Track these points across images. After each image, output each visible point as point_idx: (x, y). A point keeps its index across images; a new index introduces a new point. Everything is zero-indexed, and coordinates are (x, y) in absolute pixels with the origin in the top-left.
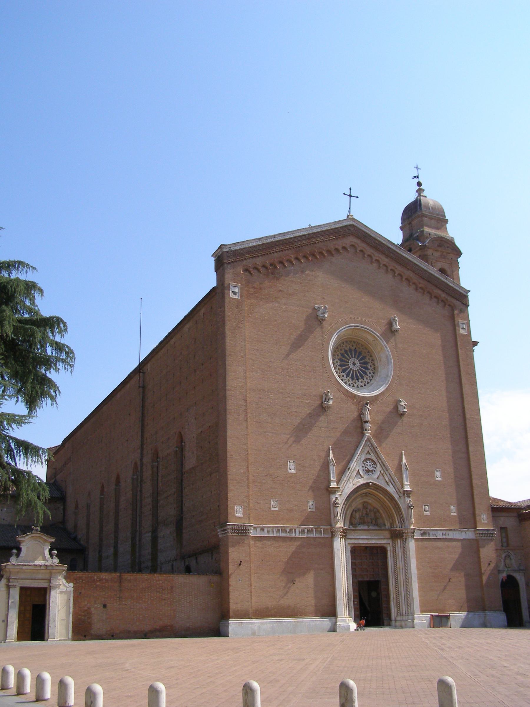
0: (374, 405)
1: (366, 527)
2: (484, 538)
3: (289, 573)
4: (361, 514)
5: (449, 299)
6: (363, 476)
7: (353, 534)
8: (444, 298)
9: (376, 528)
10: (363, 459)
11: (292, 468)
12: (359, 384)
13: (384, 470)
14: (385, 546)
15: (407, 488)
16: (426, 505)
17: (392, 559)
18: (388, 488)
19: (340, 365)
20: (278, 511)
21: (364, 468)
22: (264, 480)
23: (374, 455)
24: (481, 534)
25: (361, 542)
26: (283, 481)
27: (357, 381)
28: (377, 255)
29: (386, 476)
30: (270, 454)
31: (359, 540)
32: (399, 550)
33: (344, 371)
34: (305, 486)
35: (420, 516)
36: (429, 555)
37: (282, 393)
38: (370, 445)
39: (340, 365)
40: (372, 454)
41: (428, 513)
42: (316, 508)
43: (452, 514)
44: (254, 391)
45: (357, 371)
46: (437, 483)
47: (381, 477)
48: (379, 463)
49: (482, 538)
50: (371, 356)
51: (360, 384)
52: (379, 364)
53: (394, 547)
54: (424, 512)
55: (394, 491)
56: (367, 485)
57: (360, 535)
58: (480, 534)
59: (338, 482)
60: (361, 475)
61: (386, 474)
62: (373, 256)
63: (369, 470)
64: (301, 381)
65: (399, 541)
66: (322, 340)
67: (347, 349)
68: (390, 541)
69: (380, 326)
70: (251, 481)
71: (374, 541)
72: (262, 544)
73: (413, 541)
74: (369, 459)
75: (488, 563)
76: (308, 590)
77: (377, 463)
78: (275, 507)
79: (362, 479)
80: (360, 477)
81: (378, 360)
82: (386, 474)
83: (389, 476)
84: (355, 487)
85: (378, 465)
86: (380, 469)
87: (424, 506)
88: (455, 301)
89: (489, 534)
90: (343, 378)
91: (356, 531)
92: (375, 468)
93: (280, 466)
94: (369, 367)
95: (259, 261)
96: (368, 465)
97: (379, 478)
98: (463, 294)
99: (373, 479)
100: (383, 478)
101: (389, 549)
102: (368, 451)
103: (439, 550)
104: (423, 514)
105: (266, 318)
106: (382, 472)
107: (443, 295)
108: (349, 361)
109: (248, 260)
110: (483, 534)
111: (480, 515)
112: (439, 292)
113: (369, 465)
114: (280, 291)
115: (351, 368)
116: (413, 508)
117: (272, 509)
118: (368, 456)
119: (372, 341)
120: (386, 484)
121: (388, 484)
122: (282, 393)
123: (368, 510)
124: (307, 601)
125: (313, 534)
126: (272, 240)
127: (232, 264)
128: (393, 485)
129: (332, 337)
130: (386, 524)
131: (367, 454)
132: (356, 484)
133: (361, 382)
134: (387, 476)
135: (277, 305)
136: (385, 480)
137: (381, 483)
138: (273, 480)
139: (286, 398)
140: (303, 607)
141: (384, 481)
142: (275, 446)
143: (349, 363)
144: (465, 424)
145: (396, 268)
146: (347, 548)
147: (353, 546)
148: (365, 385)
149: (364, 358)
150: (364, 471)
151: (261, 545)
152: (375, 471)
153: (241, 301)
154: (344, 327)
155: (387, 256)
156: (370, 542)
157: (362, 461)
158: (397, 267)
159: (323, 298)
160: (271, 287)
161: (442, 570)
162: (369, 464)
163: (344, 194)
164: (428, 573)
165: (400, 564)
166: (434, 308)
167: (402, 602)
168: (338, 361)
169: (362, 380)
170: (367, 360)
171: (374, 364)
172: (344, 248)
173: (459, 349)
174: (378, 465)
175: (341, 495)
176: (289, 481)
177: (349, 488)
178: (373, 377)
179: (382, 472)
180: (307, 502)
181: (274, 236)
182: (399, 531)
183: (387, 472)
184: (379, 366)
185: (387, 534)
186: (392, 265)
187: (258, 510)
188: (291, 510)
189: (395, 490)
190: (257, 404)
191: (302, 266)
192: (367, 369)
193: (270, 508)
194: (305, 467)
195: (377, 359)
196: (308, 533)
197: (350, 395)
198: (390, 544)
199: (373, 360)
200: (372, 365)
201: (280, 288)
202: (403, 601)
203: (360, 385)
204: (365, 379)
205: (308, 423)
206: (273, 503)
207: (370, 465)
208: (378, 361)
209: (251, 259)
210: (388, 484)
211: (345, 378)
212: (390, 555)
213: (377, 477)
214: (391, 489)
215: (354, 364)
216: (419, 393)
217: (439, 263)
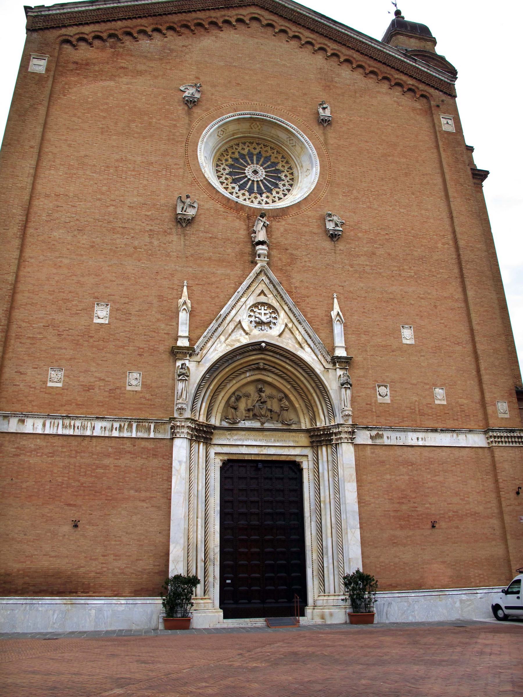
0: (279, 222)
1: (257, 425)
2: (504, 445)
3: (69, 505)
4: (249, 402)
5: (422, 86)
6: (248, 332)
7: (228, 437)
8: (413, 85)
9: (279, 426)
10: (251, 302)
12: (262, 200)
13: (293, 323)
14: (298, 459)
15: (341, 352)
16: (382, 386)
17: (312, 486)
18: (300, 353)
19: (230, 174)
20: (63, 389)
21: (253, 319)
22: (40, 333)
23: (273, 298)
24: (498, 437)
25: (244, 450)
26: (80, 337)
27: (258, 196)
28: (293, 30)
29: (297, 332)
30: (61, 292)
31: (240, 448)
32: (323, 467)
33: (234, 181)
34: (124, 346)
35: (370, 404)
36: (388, 477)
37: (99, 200)
38: (267, 281)
39: (230, 174)
40: (270, 296)
41: (388, 400)
42: (144, 385)
43: (437, 402)
44: (47, 196)
45: (260, 183)
46: (404, 349)
47: (287, 334)
48: (283, 312)
49: (500, 444)
50: (287, 162)
51: (265, 199)
52: (300, 172)
53: (317, 462)
54: (379, 397)
55: (313, 359)
57: (243, 440)
58: (495, 437)
60: (244, 330)
61: (298, 329)
62: (288, 30)
63: (262, 321)
64: (141, 184)
65: (324, 449)
66: (187, 129)
67: (245, 152)
68: (308, 451)
69: (297, 116)
70: (14, 335)
71: (272, 451)
72: (17, 448)
73: (351, 448)
74: (263, 304)
75: (515, 492)
76: (109, 541)
77: (279, 311)
79: (247, 337)
80: (243, 333)
81: (298, 166)
82: (298, 329)
83: (303, 332)
84: (229, 349)
85: (282, 314)
86: (286, 321)
87: (379, 386)
88: (432, 91)
89: (515, 437)
90: (233, 190)
91: (235, 432)
92: (275, 318)
93: (78, 312)
94: (283, 177)
95: (87, 29)
96: (259, 313)
97: (283, 336)
98: (445, 82)
100: (292, 336)
101: (307, 466)
102: (262, 290)
103: (410, 468)
104: (376, 401)
105: (89, 100)
106: (290, 325)
107: (410, 82)
108: (247, 169)
109: (70, 29)
110: (501, 437)
111: (495, 405)
112: (404, 78)
113: (263, 314)
114: (122, 68)
115: (249, 177)
116: (349, 386)
117: (50, 384)
118: (263, 299)
119: (286, 139)
120: (297, 346)
121: (302, 347)
122: (99, 200)
123: (263, 395)
124: (102, 563)
125: (131, 431)
127: (41, 32)
128: (311, 348)
129: (207, 126)
130: (302, 420)
131: (259, 295)
132: (234, 345)
133: (268, 197)
134: (300, 332)
135: (112, 83)
136: (296, 339)
138: (58, 335)
139: (108, 206)
140: (92, 574)
141: (294, 341)
142: (73, 280)
143: (246, 171)
144: (459, 255)
145: (329, 47)
146: (212, 461)
147: (226, 458)
149: (274, 164)
150: (253, 323)
151: (13, 450)
152: (275, 324)
153: (46, 76)
155: (313, 31)
156: (265, 451)
157: (248, 307)
158: (329, 45)
160: (107, 63)
161: (416, 505)
162: (263, 312)
164: (385, 511)
165: (325, 493)
166: (395, 99)
167: (328, 567)
168: (227, 168)
169: (269, 194)
170: (279, 167)
171: (292, 174)
173: (441, 150)
174: (282, 314)
175: (199, 362)
176: (92, 337)
177: (216, 352)
178: (289, 190)
179: (290, 325)
180: (125, 373)
182: (324, 429)
183: (299, 327)
184: (300, 174)
185: (303, 440)
186: (319, 41)
187: (19, 385)
188: (89, 388)
189: (315, 357)
190: (49, 215)
191: (165, 39)
192: (280, 179)
193: (45, 382)
194: (130, 314)
195: (297, 165)
196: (120, 430)
197: (233, 205)
198: (307, 456)
199: (290, 168)
200: (288, 175)
201: (122, 65)
202: (331, 566)
203: (264, 201)
204: (274, 193)
205: (145, 245)
206: (53, 374)
207: (265, 314)
208: (299, 169)
209: (75, 27)
210: (302, 347)
211: (237, 191)
212: (307, 477)
213: (278, 334)
215: (255, 172)
216: (369, 207)
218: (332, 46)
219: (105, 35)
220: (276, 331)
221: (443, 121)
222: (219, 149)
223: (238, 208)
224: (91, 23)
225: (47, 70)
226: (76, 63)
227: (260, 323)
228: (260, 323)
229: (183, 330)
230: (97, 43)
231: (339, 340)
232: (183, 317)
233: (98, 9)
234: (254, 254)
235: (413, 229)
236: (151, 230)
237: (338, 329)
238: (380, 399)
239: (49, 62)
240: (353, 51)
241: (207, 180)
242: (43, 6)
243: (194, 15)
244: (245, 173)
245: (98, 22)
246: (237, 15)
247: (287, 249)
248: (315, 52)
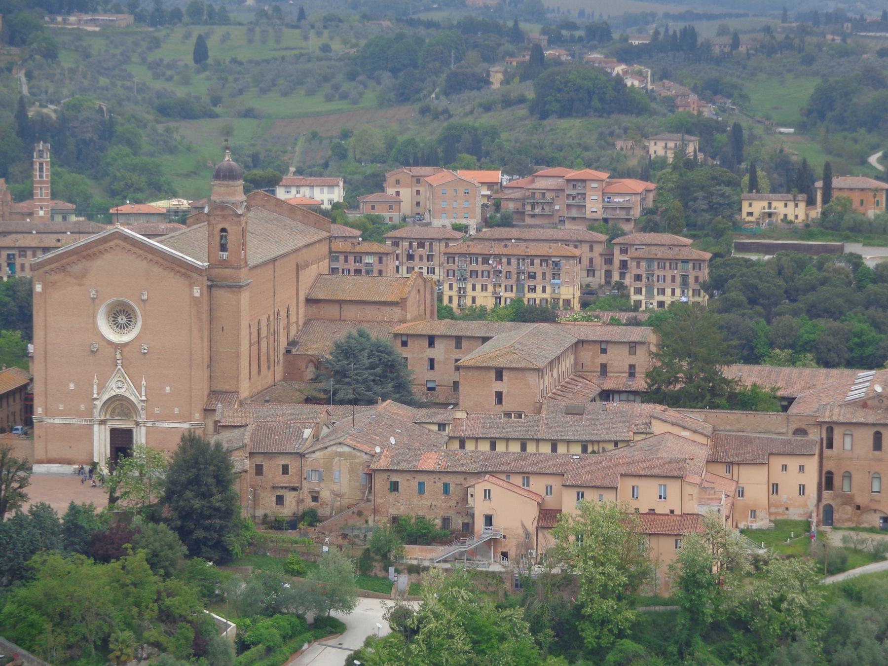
11: (72, 386)
15: (144, 398)
18: (131, 398)
28: (134, 249)
42: (86, 408)
56: (117, 396)
59: (98, 394)
78: (61, 407)
95: (53, 266)
99: (121, 392)
107: (183, 271)
118: (120, 379)
137: (127, 395)
172: (111, 248)
214: (132, 398)
218: (150, 256)
220: (123, 390)
221: (195, 291)
223: (110, 343)
227: (119, 388)
228: (119, 388)
229: (95, 392)
231: (143, 393)
232: (95, 387)
234: (117, 363)
237: (143, 389)
238: (156, 412)
243: (92, 250)
248: (143, 260)
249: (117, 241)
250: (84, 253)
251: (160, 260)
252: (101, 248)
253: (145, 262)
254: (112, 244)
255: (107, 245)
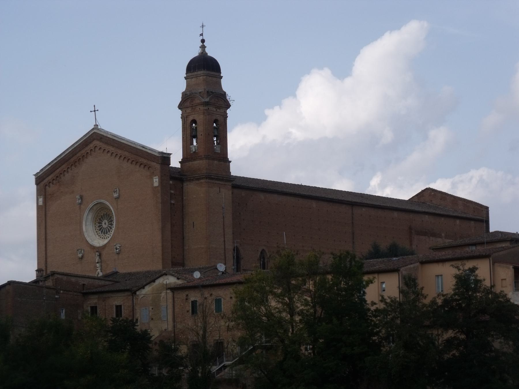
8: (146, 163)
28: (108, 148)
33: (100, 230)
67: (102, 215)
95: (50, 177)
107: (145, 161)
109: (46, 179)
126: (55, 161)
145: (118, 153)
148: (103, 238)
154: (91, 204)
155: (113, 146)
158: (119, 152)
159: (81, 189)
163: (91, 111)
181: (56, 159)
209: (47, 178)
217: (190, 116)
218: (120, 152)
219: (55, 178)
221: (155, 180)
222: (94, 216)
224: (51, 174)
225: (43, 203)
226: (50, 195)
230: (54, 182)
233: (52, 166)
235: (141, 242)
236: (74, 263)
239: (43, 199)
240: (126, 152)
241: (86, 238)
242: (37, 173)
244: (102, 225)
245: (52, 173)
246: (90, 148)
247: (106, 262)
249: (96, 143)
250: (72, 160)
251: (127, 154)
252: (83, 151)
253: (117, 159)
254: (91, 146)
255: (88, 149)
